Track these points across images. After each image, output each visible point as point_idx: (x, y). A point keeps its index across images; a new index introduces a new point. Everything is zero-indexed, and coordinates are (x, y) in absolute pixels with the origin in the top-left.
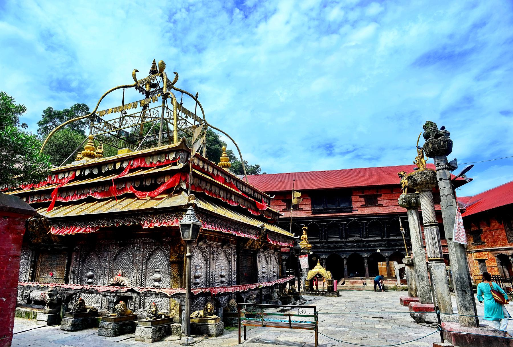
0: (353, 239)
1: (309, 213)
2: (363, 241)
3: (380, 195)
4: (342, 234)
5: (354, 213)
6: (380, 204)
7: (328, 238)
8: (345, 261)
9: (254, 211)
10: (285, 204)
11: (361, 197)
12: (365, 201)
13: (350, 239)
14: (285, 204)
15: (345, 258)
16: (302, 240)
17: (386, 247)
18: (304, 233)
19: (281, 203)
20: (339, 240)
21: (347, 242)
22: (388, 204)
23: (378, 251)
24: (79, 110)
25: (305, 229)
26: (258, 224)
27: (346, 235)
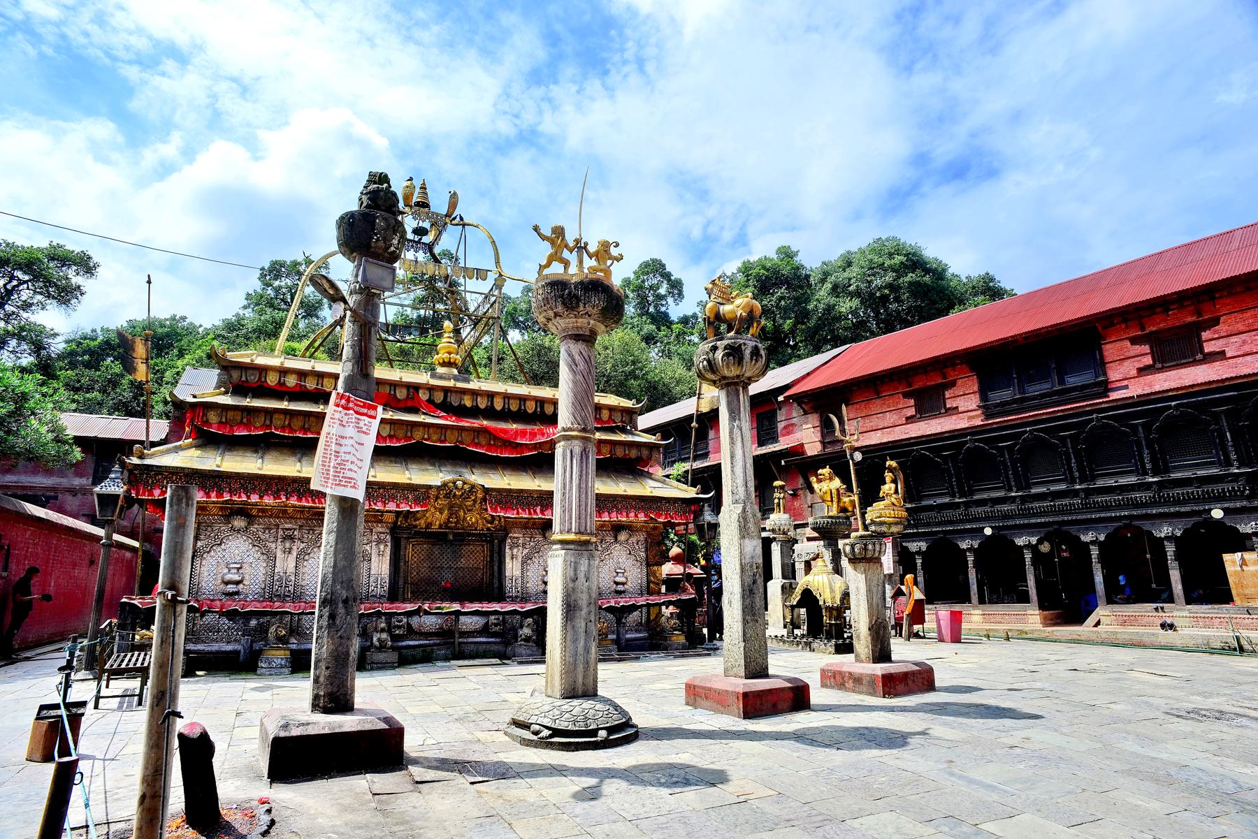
0: (1111, 482)
1: (973, 417)
2: (1148, 486)
3: (1215, 322)
4: (1070, 469)
5: (1114, 396)
6: (1211, 354)
7: (1029, 487)
8: (1095, 552)
10: (912, 402)
11: (1134, 341)
12: (1152, 353)
13: (1100, 483)
14: (912, 402)
15: (1093, 543)
16: (883, 499)
17: (1243, 497)
19: (903, 402)
20: (1063, 487)
21: (1088, 492)
22: (1247, 348)
23: (1217, 514)
24: (647, 273)
25: (891, 470)
27: (1081, 470)
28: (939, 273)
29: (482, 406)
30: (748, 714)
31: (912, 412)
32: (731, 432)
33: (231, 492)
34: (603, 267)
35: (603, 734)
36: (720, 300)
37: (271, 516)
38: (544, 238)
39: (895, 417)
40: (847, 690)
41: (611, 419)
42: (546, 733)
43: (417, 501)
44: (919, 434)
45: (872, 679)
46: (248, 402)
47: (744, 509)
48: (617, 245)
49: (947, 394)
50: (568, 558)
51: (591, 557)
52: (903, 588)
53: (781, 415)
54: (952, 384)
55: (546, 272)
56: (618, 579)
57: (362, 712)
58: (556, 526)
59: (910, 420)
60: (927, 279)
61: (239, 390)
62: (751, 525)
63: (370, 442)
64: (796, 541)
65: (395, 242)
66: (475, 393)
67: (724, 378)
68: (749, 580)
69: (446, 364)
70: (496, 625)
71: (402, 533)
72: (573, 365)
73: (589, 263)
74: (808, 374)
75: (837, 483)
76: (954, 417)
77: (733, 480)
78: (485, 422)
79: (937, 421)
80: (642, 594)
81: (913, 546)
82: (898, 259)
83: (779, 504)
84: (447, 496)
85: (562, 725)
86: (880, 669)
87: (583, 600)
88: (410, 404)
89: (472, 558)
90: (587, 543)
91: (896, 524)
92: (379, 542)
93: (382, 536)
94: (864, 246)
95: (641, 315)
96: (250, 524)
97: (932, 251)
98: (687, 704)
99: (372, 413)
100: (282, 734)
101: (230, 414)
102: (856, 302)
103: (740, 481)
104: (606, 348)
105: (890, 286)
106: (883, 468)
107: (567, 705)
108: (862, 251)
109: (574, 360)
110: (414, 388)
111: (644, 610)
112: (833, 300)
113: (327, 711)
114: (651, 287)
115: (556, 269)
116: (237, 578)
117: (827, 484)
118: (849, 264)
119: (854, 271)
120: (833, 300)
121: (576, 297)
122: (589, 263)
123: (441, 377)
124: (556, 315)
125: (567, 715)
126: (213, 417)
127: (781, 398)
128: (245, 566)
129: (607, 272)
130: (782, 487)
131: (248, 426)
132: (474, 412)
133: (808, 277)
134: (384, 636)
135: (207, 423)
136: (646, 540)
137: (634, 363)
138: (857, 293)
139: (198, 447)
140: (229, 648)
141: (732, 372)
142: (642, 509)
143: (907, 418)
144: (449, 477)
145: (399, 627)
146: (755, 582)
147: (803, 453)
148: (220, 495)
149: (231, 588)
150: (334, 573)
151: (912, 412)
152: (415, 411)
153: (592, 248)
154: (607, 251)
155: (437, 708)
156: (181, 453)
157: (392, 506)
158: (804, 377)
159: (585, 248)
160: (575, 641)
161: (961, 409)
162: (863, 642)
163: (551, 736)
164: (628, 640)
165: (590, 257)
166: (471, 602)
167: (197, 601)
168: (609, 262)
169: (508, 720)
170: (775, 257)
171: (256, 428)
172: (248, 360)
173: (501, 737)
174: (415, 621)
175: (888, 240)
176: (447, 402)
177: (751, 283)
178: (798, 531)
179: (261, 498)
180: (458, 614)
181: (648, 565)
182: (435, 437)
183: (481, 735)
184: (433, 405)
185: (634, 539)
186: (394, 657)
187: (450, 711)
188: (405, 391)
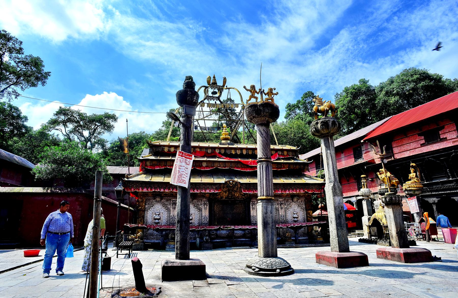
9: (242, 168)
10: (423, 137)
14: (423, 137)
16: (410, 180)
18: (412, 171)
24: (307, 97)
25: (413, 167)
26: (222, 181)
28: (438, 80)
29: (239, 153)
30: (340, 267)
31: (423, 141)
32: (327, 155)
33: (155, 188)
34: (270, 98)
35: (278, 271)
36: (319, 105)
37: (168, 196)
38: (247, 90)
39: (415, 144)
40: (388, 259)
41: (288, 155)
42: (257, 270)
43: (216, 189)
44: (428, 151)
45: (399, 255)
46: (158, 158)
47: (334, 185)
48: (275, 89)
49: (440, 133)
50: (263, 205)
51: (272, 205)
52: (424, 218)
53: (363, 148)
54: (443, 128)
55: (249, 102)
56: (294, 216)
57: (192, 259)
58: (259, 194)
59: (422, 145)
60: (432, 83)
61: (155, 154)
62: (337, 191)
63: (190, 167)
64: (375, 200)
65: (195, 98)
66: (235, 149)
67: (322, 134)
68: (338, 213)
69: (226, 139)
70: (248, 234)
71: (212, 200)
72: (261, 134)
73: (265, 97)
74: (374, 130)
75: (389, 174)
76: (445, 142)
77: (329, 174)
78: (240, 159)
79: (437, 144)
80: (304, 222)
81: (431, 200)
82: (415, 77)
83: (364, 185)
84: (227, 187)
85: (263, 267)
86: (402, 250)
87: (270, 221)
88: (213, 155)
89: (239, 209)
90: (271, 199)
91: (417, 190)
92: (205, 204)
93: (206, 202)
94: (398, 73)
95: (306, 114)
96: (162, 199)
97: (432, 71)
98: (317, 262)
99: (190, 157)
100: (166, 265)
101: (154, 162)
102: (397, 98)
103: (332, 173)
104: (291, 128)
105: (413, 89)
106: (409, 166)
107: (265, 260)
108: (398, 76)
109: (261, 133)
110: (214, 148)
111: (306, 228)
112: (386, 98)
113: (180, 259)
114: (309, 103)
115: (253, 101)
116: (158, 217)
117: (384, 175)
118: (392, 82)
119: (395, 85)
120: (386, 98)
121: (260, 110)
122: (265, 97)
123: (223, 144)
124: (254, 117)
125: (265, 263)
126: (148, 163)
127: (362, 141)
128: (161, 214)
129: (272, 99)
130: (364, 177)
131: (159, 166)
132: (236, 156)
133: (374, 90)
134: (207, 238)
135: (146, 166)
136: (305, 200)
137: (302, 132)
138: (397, 94)
139: (144, 174)
140: (157, 241)
141: (325, 131)
142: (302, 188)
143: (421, 145)
144: (227, 180)
145: (213, 235)
146: (341, 213)
147: (375, 163)
148: (151, 190)
149: (157, 221)
150: (181, 212)
151: (423, 141)
152: (214, 157)
153: (266, 91)
154: (272, 92)
155: (223, 262)
156: (139, 176)
157: (208, 191)
158: (372, 132)
159: (263, 91)
160: (268, 236)
161: (448, 138)
162: (394, 239)
163: (259, 271)
164: (299, 240)
165: (265, 95)
166: (238, 225)
167: (146, 225)
168: (273, 96)
169: (245, 266)
170: (359, 84)
171: (162, 167)
172: (158, 144)
173: (243, 271)
174: (218, 232)
175: (409, 69)
176: (226, 152)
177: (349, 96)
178: (375, 195)
179: (164, 190)
180: (233, 229)
181: (307, 210)
182: (222, 166)
183: (235, 271)
184: (221, 155)
185: (300, 201)
186: (211, 245)
187: (227, 263)
188: (211, 150)
